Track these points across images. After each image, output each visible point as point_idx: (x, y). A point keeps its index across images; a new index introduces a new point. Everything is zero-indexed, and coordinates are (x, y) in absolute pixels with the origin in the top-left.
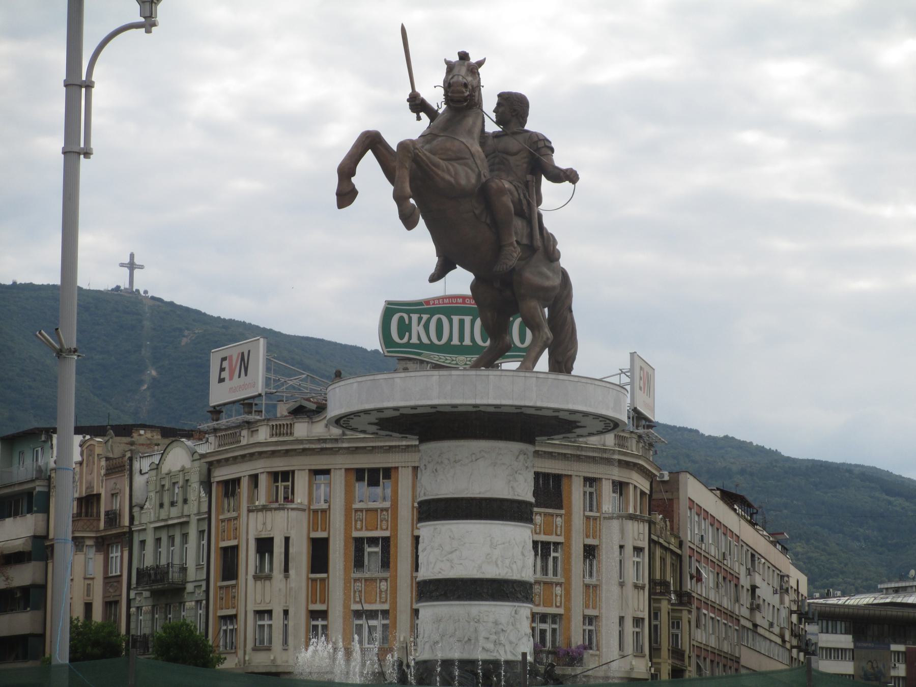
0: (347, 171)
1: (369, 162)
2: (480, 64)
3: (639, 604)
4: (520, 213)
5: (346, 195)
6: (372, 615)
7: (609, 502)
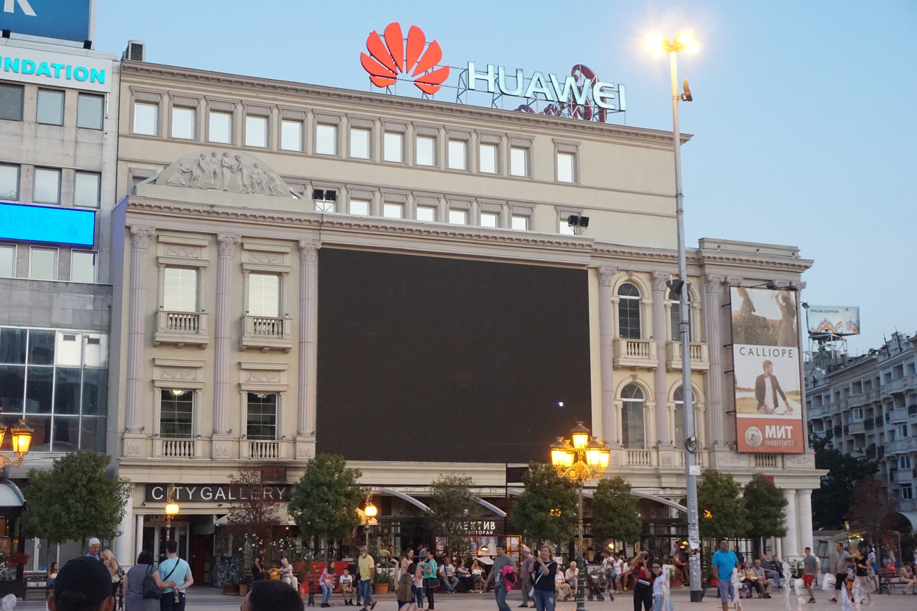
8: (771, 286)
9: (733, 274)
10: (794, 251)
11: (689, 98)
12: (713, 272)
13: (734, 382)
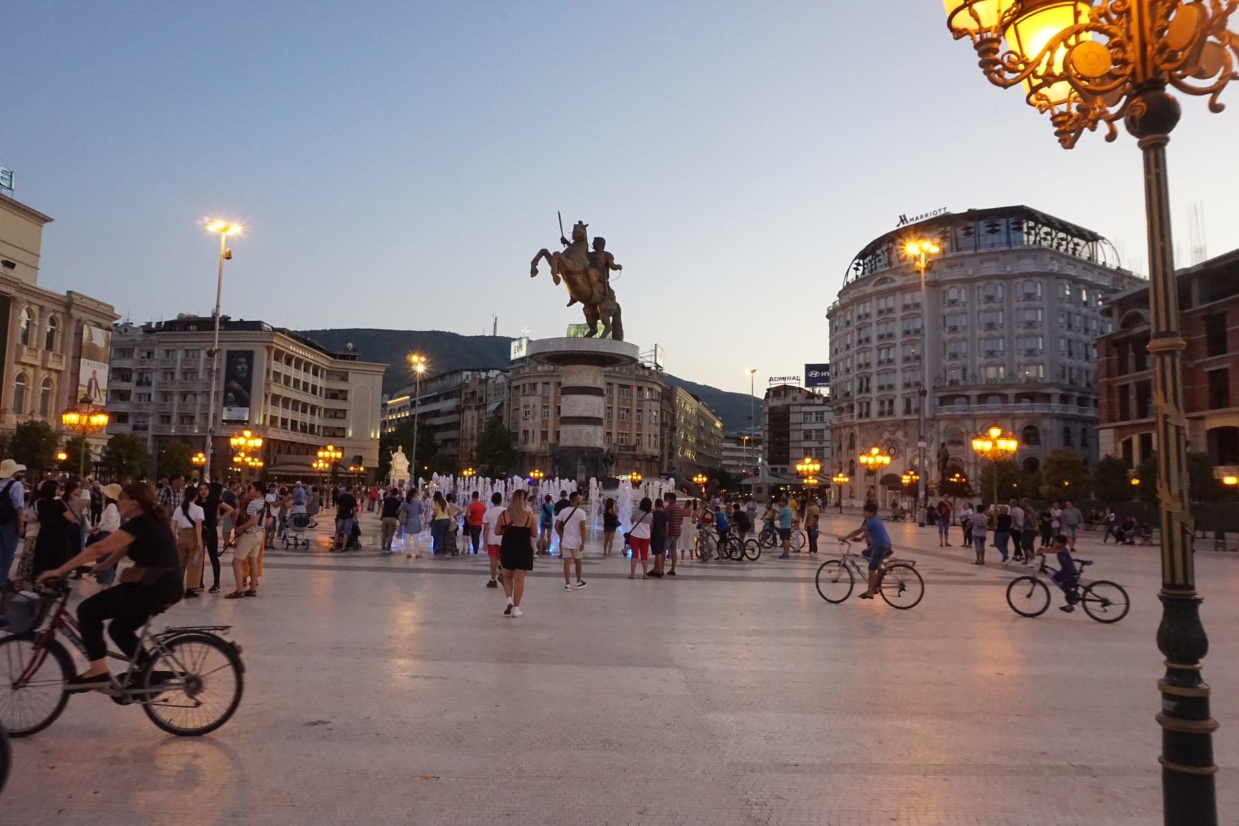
0: (535, 263)
1: (543, 260)
3: (658, 430)
4: (600, 281)
5: (534, 272)
7: (647, 395)
8: (99, 325)
9: (85, 316)
10: (112, 308)
11: (229, 257)
12: (76, 313)
13: (78, 379)
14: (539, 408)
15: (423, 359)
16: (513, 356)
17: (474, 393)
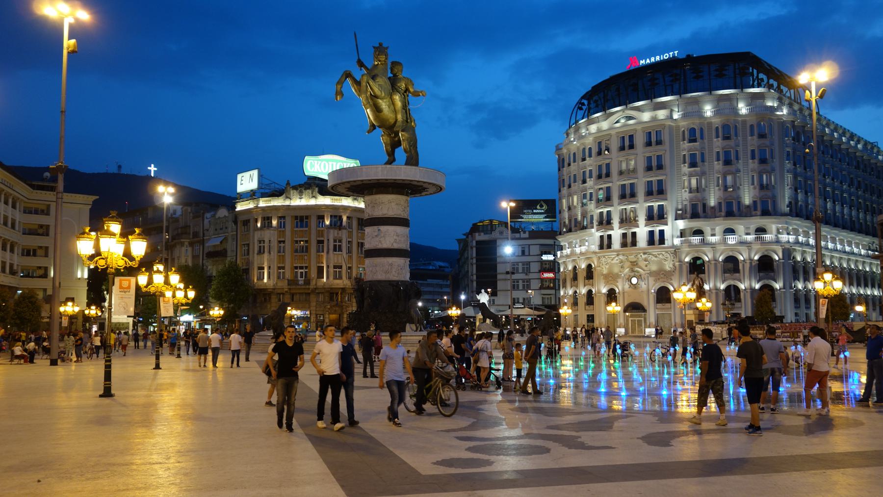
2: (387, 48)
6: (301, 268)
14: (275, 244)
15: (171, 190)
16: (241, 189)
17: (187, 227)
